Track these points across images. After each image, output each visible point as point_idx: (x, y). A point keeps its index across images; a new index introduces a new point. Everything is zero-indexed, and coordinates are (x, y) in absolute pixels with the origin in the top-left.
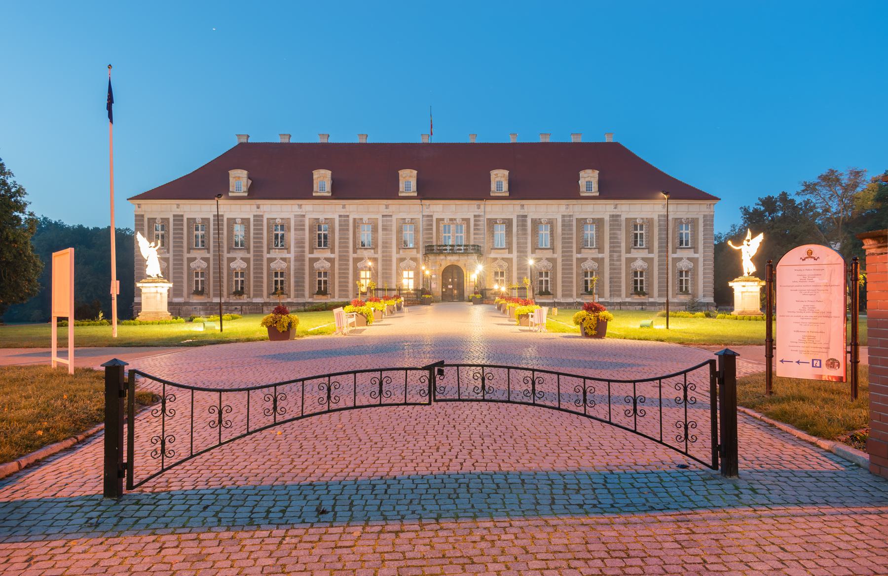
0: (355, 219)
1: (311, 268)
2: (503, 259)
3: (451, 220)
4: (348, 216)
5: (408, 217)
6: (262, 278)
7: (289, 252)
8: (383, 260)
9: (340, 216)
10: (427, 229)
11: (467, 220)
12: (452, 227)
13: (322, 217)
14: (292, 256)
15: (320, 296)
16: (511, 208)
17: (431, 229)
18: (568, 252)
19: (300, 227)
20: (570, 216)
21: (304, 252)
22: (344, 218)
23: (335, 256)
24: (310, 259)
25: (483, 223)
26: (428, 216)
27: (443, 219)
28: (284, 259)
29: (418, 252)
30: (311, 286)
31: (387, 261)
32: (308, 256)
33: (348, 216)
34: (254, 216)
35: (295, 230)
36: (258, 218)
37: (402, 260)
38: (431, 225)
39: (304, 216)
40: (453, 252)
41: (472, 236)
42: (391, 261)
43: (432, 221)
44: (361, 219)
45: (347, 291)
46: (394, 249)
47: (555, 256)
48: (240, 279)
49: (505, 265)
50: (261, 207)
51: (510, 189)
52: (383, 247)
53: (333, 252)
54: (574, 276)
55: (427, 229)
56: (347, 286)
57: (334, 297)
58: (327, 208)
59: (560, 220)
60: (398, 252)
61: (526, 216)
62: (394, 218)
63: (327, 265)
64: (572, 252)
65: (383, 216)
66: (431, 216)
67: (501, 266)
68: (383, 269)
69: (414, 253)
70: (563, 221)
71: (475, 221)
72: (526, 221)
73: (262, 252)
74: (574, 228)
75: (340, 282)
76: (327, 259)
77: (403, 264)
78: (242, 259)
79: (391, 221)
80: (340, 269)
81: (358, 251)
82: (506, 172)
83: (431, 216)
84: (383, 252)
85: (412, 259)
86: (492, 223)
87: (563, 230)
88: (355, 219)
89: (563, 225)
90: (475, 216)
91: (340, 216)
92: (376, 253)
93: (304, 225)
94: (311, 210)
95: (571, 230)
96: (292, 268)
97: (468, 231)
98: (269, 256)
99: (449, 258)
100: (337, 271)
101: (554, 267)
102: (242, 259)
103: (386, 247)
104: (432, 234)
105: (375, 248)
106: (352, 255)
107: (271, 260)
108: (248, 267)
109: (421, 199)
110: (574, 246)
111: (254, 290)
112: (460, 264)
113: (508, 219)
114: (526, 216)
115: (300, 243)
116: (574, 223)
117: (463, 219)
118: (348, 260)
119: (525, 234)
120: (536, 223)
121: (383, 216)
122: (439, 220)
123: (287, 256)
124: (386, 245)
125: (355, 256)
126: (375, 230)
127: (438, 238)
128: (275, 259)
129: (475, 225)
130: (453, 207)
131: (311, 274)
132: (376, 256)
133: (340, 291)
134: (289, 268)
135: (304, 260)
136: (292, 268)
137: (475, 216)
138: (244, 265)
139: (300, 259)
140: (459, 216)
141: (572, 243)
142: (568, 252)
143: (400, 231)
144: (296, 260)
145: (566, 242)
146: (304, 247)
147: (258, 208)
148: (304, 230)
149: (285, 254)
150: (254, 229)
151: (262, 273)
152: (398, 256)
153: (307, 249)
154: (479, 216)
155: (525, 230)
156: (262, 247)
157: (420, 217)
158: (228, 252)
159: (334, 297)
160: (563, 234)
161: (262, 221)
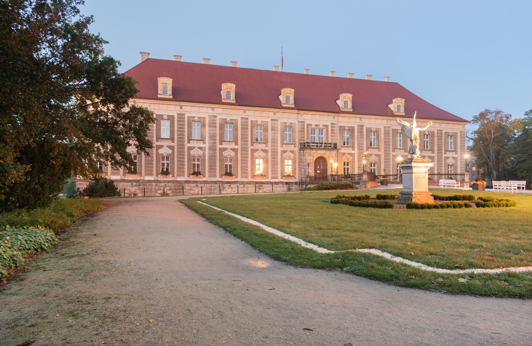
0: (252, 121)
1: (221, 155)
2: (349, 154)
3: (316, 125)
4: (247, 119)
5: (288, 122)
6: (184, 162)
7: (204, 143)
8: (272, 152)
9: (242, 118)
10: (301, 131)
11: (326, 126)
12: (317, 131)
13: (228, 118)
14: (207, 146)
15: (228, 177)
16: (353, 120)
17: (304, 131)
18: (387, 151)
19: (213, 125)
20: (389, 127)
21: (215, 143)
22: (245, 120)
23: (239, 147)
24: (220, 149)
25: (337, 129)
26: (302, 122)
27: (311, 125)
28: (200, 148)
29: (295, 147)
30: (221, 169)
31: (274, 152)
32: (218, 146)
33: (247, 119)
34: (178, 114)
35: (209, 126)
36: (181, 116)
37: (284, 152)
38: (304, 128)
39: (216, 116)
40: (326, 148)
41: (330, 138)
42: (277, 152)
43: (304, 125)
44: (257, 121)
45: (247, 173)
46: (279, 144)
47: (380, 153)
48: (165, 162)
49: (350, 158)
50: (183, 107)
51: (353, 107)
52: (272, 142)
53: (236, 143)
54: (391, 166)
55: (301, 131)
56: (247, 170)
57: (237, 178)
58: (233, 112)
59: (383, 130)
60: (282, 147)
61: (363, 126)
62: (279, 122)
63: (233, 154)
64: (389, 151)
65: (272, 120)
66: (304, 122)
67: (348, 159)
68: (272, 158)
69: (292, 147)
70: (385, 130)
71: (332, 127)
72: (363, 129)
73: (184, 142)
74: (391, 135)
75: (242, 167)
76: (233, 150)
77: (285, 155)
78: (168, 146)
79: (277, 124)
80: (242, 157)
81: (255, 144)
82: (351, 96)
83: (304, 122)
84: (272, 146)
85: (292, 152)
86: (342, 129)
87: (385, 136)
88: (252, 121)
89: (385, 133)
90: (332, 124)
91: (242, 118)
92: (267, 146)
93: (216, 123)
94: (221, 113)
95: (389, 136)
96: (207, 155)
97: (327, 134)
98: (189, 145)
99: (319, 152)
100: (239, 158)
101: (380, 160)
102: (168, 146)
103: (274, 142)
104: (304, 134)
105: (266, 143)
106: (250, 148)
107: (190, 148)
108: (173, 153)
109: (299, 110)
110: (391, 147)
111: (178, 171)
112: (325, 156)
113: (352, 127)
114: (363, 126)
115: (213, 137)
116: (391, 132)
117: (324, 126)
118: (248, 151)
119: (363, 138)
120: (369, 131)
121: (272, 120)
122: (308, 125)
123: (203, 146)
124: (274, 141)
125: (252, 148)
126: (266, 130)
127: (308, 137)
128: (194, 148)
129: (332, 130)
130: (318, 117)
131: (221, 160)
132: (267, 148)
133: (242, 173)
134: (204, 155)
135: (216, 150)
136: (207, 155)
137: (332, 124)
138: (170, 151)
139: (212, 148)
140: (321, 124)
141: (389, 145)
142: (387, 151)
143: (283, 132)
144: (209, 149)
145: (387, 144)
146: (215, 140)
147: (181, 108)
148: (215, 127)
149: (201, 145)
150: (178, 125)
151: (184, 158)
152: (282, 149)
153: (218, 141)
154: (334, 124)
155: (362, 135)
156: (184, 138)
157: (296, 122)
158: (157, 141)
159: (237, 178)
160: (385, 139)
161: (184, 118)
